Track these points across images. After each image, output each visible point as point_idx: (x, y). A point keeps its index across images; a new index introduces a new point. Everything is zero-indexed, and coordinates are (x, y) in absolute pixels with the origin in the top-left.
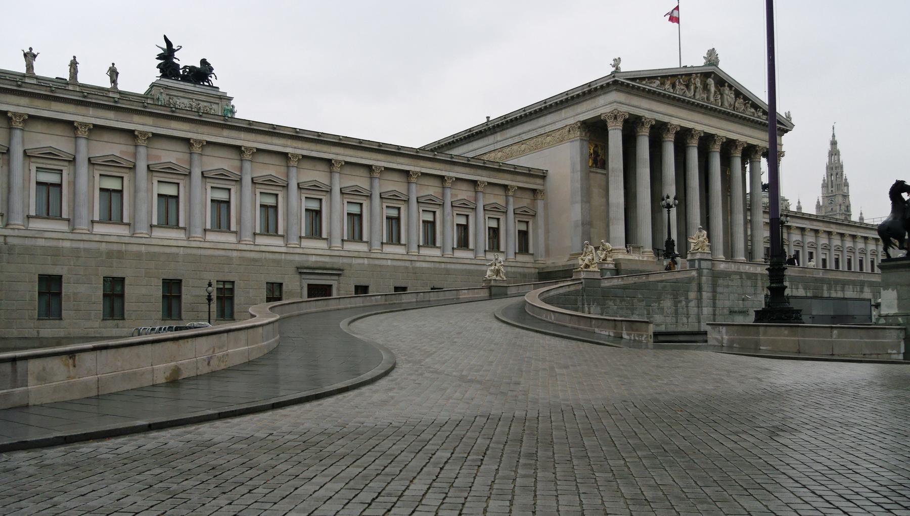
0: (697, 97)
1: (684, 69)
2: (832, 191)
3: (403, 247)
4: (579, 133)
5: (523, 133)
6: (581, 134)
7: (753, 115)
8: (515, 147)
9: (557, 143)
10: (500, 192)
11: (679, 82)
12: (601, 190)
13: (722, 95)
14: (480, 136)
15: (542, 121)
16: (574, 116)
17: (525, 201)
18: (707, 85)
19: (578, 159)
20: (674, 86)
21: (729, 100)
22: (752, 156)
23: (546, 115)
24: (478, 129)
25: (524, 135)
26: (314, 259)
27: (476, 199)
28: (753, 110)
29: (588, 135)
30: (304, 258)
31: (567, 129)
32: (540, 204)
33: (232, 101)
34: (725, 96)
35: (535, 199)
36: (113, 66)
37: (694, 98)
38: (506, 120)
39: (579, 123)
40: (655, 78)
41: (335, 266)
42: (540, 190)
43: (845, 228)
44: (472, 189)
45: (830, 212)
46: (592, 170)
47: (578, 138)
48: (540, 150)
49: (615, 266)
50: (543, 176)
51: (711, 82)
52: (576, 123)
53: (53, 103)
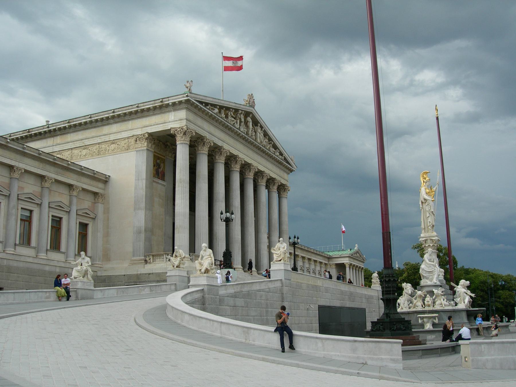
0: (242, 130)
4: (146, 144)
5: (86, 139)
6: (148, 145)
7: (274, 154)
8: (76, 152)
9: (122, 151)
10: (64, 190)
11: (231, 114)
12: (161, 200)
13: (255, 132)
14: (39, 137)
15: (106, 129)
16: (142, 128)
17: (87, 203)
18: (247, 122)
19: (143, 168)
20: (227, 117)
21: (261, 137)
23: (111, 124)
25: (87, 140)
27: (41, 196)
29: (153, 146)
31: (134, 139)
32: (100, 208)
34: (258, 134)
37: (239, 130)
38: (69, 124)
39: (147, 134)
43: (305, 252)
44: (39, 184)
46: (155, 180)
47: (146, 148)
48: (103, 156)
49: (187, 274)
50: (105, 180)
51: (249, 119)
52: (144, 134)
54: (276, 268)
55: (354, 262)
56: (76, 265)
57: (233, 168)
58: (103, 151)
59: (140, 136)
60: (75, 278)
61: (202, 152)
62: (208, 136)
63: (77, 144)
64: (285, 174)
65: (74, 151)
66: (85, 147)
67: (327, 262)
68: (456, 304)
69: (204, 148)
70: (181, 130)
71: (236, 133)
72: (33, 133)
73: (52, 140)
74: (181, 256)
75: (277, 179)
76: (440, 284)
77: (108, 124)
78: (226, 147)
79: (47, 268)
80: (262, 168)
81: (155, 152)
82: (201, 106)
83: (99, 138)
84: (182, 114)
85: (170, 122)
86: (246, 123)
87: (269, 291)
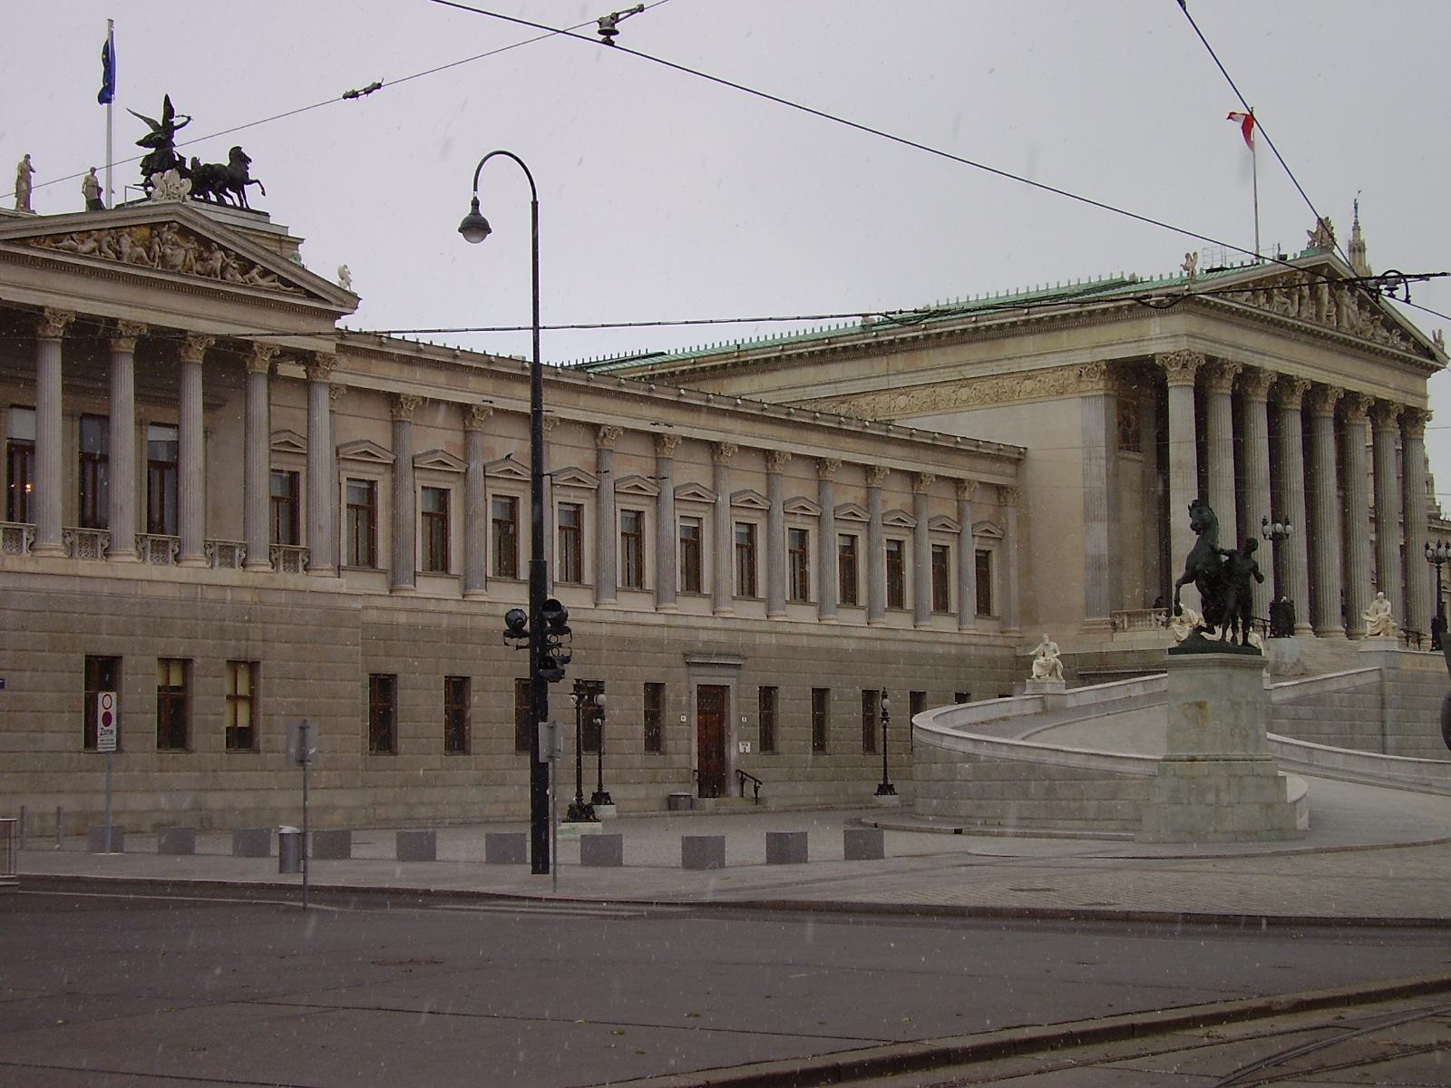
3: (813, 608)
4: (1102, 384)
8: (944, 391)
9: (1050, 395)
13: (1337, 306)
14: (851, 354)
15: (1010, 346)
17: (981, 509)
20: (1269, 299)
21: (1352, 316)
22: (1380, 421)
23: (1021, 335)
24: (851, 341)
25: (968, 367)
26: (704, 636)
31: (1076, 371)
32: (1011, 513)
33: (300, 246)
34: (1345, 308)
35: (1001, 506)
36: (93, 174)
50: (1017, 458)
52: (1097, 362)
53: (374, 361)
56: (1035, 657)
57: (1285, 404)
58: (1006, 392)
59: (1089, 367)
60: (1038, 677)
61: (1219, 391)
62: (1230, 354)
63: (946, 375)
64: (1419, 381)
65: (938, 390)
66: (964, 382)
69: (1224, 381)
70: (1178, 358)
71: (1294, 328)
72: (838, 345)
73: (885, 363)
74: (1190, 622)
75: (1394, 401)
78: (1270, 365)
79: (939, 649)
80: (1353, 386)
82: (1217, 300)
83: (995, 364)
84: (1178, 323)
85: (1151, 339)
87: (1357, 691)
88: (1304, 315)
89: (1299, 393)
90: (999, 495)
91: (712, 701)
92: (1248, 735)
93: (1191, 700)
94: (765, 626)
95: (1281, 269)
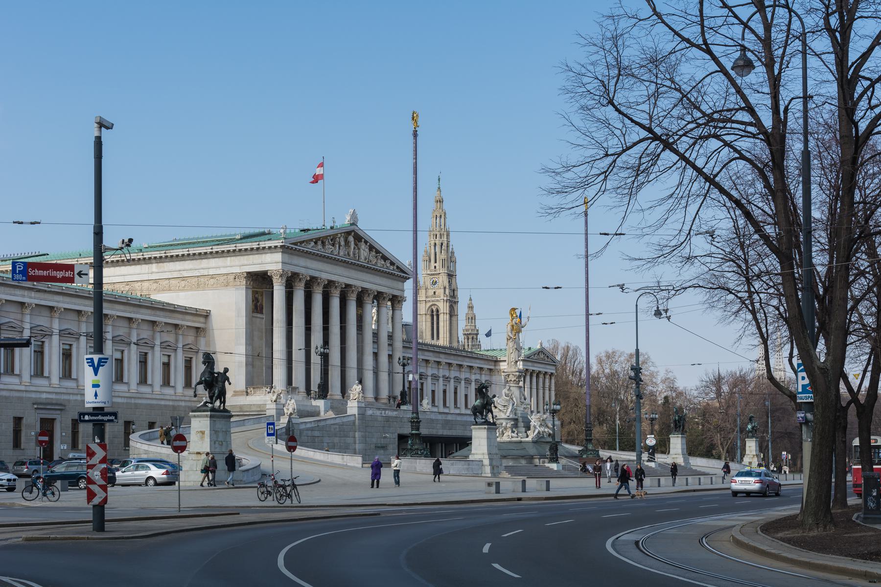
0: (342, 253)
1: (332, 231)
2: (435, 267)
4: (245, 282)
6: (246, 283)
8: (173, 282)
11: (329, 242)
13: (359, 249)
14: (131, 262)
15: (205, 263)
16: (240, 266)
22: (380, 302)
25: (185, 272)
26: (44, 396)
27: (153, 338)
28: (383, 263)
30: (38, 395)
31: (233, 277)
34: (362, 251)
40: (311, 240)
41: (59, 402)
42: (203, 329)
45: (432, 297)
46: (254, 315)
50: (206, 315)
51: (351, 239)
54: (351, 406)
55: (532, 366)
66: (184, 278)
67: (492, 367)
68: (527, 436)
76: (516, 417)
77: (206, 258)
78: (325, 276)
79: (163, 403)
80: (366, 285)
81: (253, 288)
82: (296, 247)
86: (347, 243)
88: (340, 255)
89: (339, 290)
90: (197, 332)
91: (47, 427)
92: (222, 445)
93: (199, 430)
94: (76, 391)
95: (332, 232)
